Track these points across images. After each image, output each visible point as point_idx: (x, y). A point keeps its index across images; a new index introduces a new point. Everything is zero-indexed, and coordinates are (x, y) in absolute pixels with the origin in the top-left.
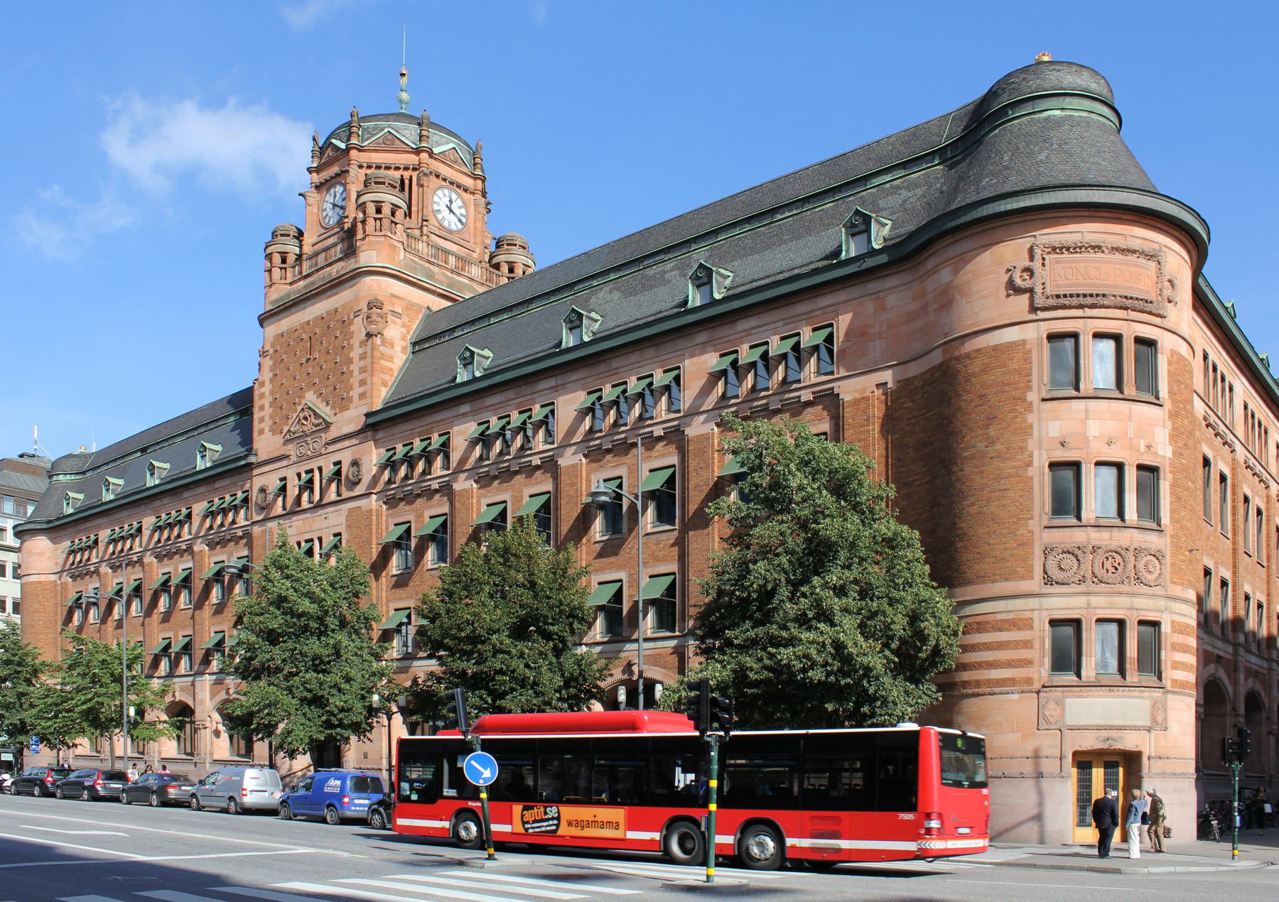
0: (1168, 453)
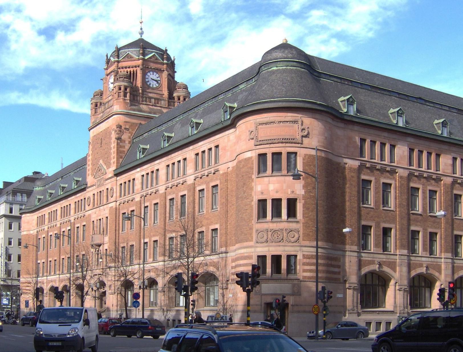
0: (303, 192)
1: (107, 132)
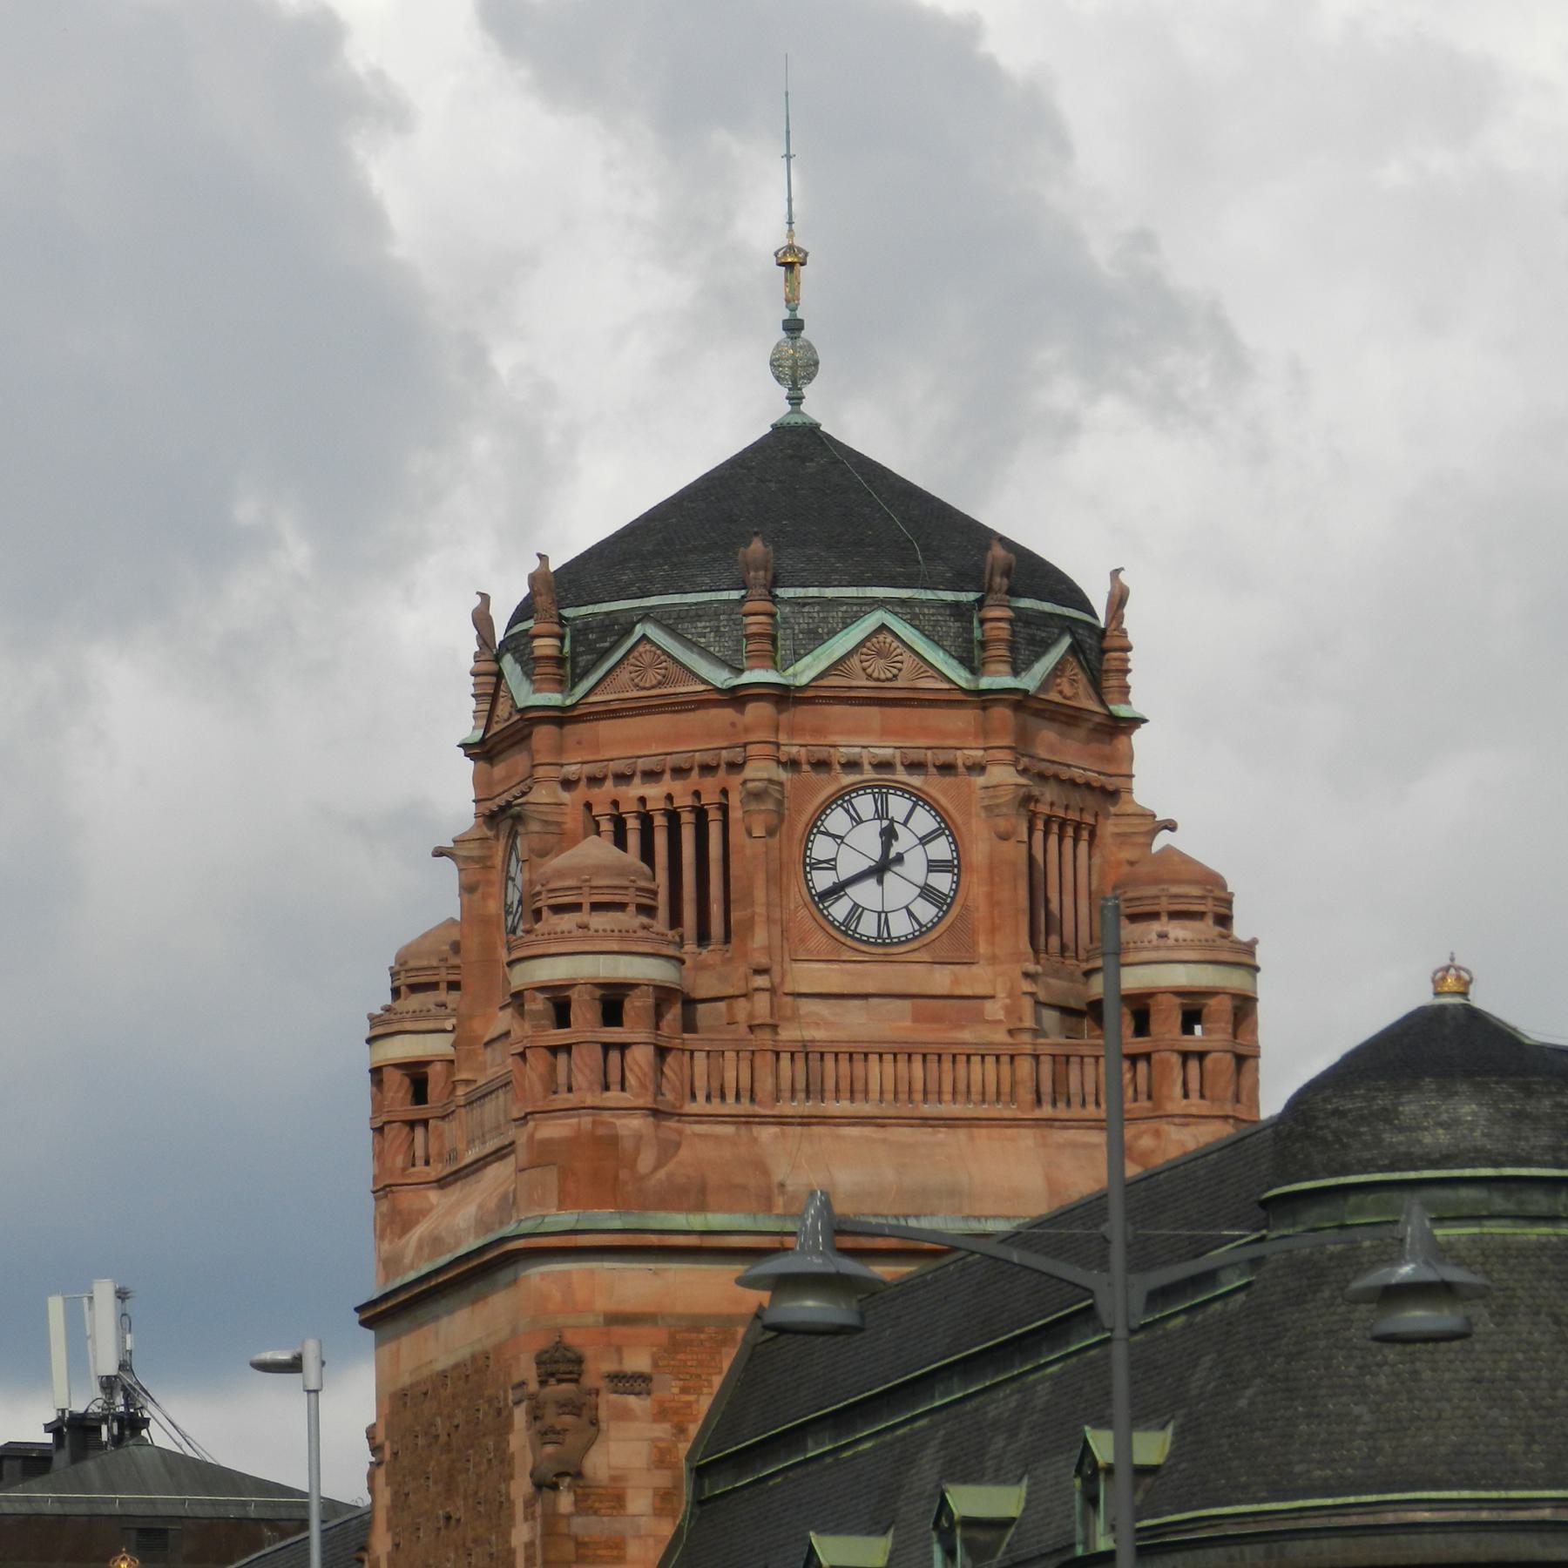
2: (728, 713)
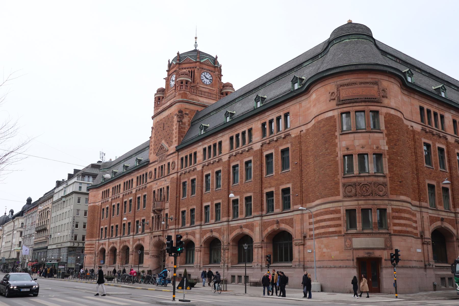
0: (386, 148)
1: (169, 118)
2: (194, 64)
